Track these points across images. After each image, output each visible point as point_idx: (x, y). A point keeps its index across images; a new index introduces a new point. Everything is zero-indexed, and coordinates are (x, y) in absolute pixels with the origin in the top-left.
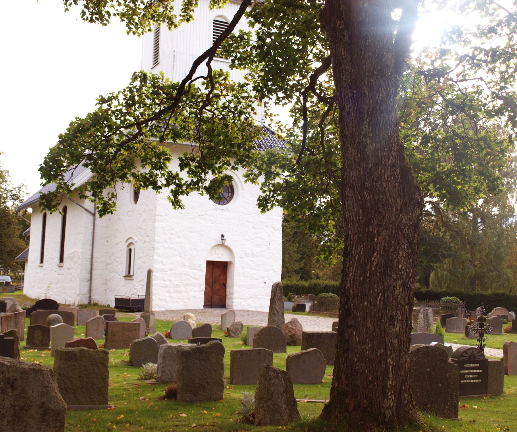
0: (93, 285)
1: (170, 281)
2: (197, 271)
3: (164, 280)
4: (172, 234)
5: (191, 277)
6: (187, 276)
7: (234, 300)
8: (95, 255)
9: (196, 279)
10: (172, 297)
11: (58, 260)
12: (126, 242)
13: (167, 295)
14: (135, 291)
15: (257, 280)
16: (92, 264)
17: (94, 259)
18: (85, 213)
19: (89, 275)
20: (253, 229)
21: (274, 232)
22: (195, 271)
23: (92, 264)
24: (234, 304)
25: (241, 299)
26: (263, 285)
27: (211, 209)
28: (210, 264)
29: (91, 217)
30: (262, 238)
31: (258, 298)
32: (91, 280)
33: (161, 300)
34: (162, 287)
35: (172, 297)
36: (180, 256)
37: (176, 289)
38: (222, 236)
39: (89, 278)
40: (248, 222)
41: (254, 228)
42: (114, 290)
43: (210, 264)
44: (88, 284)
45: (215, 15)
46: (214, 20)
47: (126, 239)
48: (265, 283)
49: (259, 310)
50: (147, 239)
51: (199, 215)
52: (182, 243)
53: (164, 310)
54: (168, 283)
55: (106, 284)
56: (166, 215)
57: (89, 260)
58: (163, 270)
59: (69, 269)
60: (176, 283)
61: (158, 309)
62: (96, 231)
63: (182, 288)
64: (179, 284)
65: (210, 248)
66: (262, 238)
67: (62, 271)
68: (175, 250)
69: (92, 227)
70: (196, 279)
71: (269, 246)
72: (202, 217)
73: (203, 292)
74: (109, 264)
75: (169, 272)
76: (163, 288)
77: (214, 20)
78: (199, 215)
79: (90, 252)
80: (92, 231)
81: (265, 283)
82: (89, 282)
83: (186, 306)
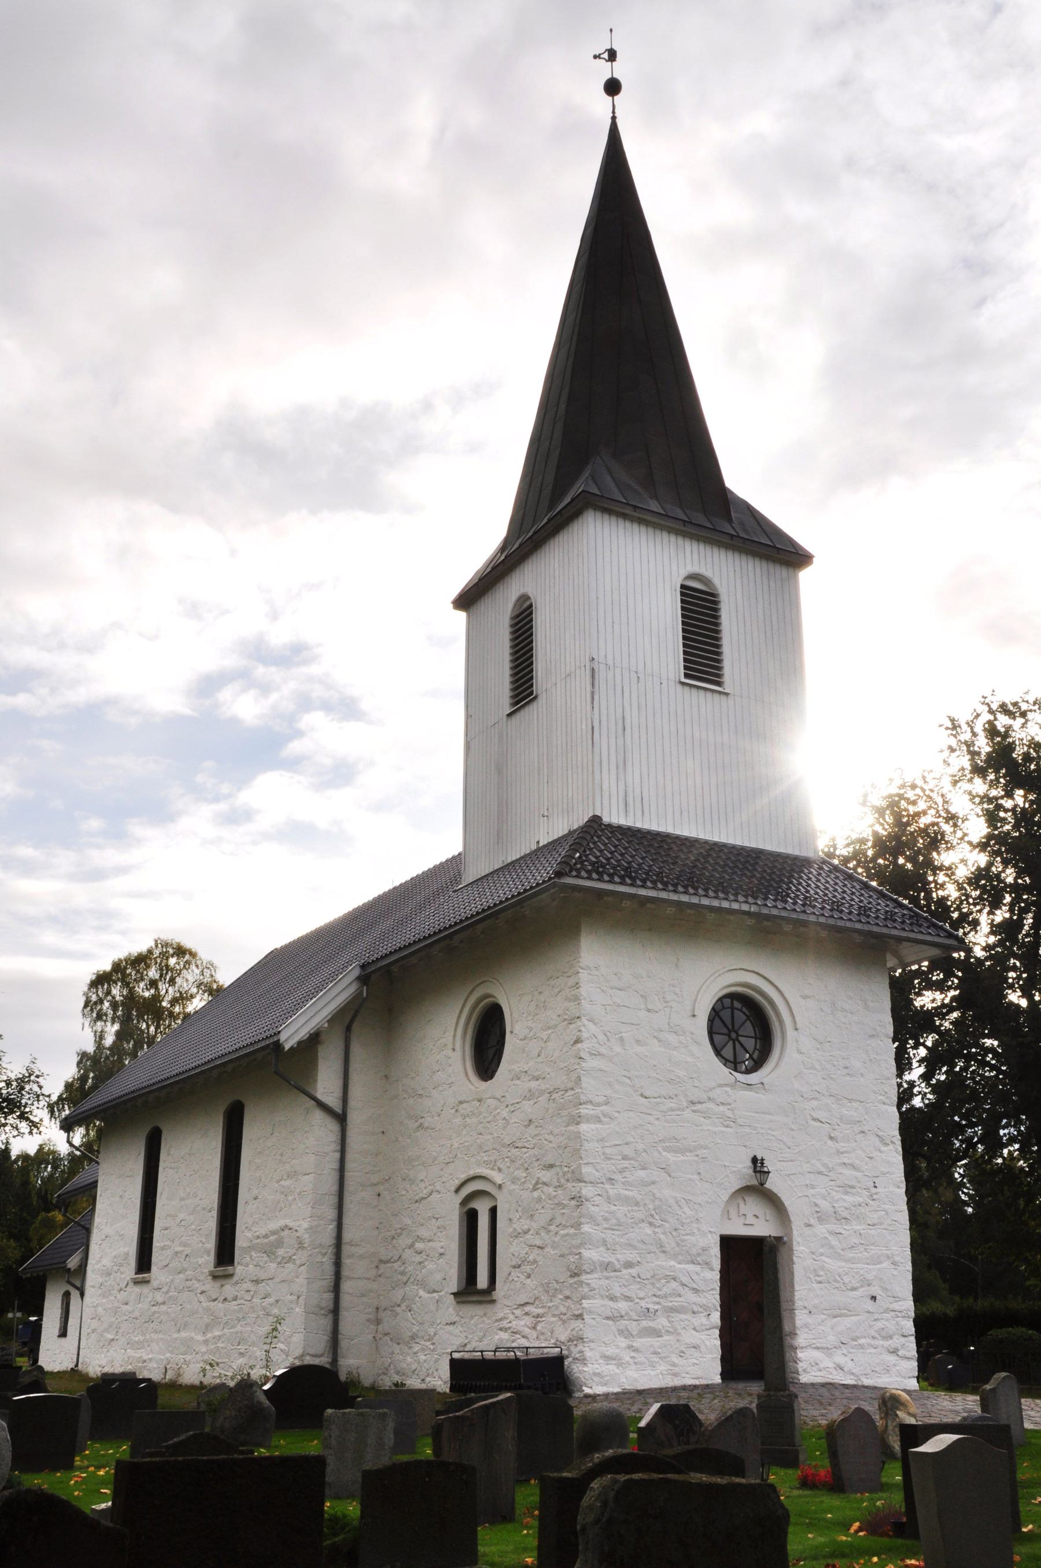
0: (344, 1327)
1: (628, 1298)
2: (698, 1268)
3: (613, 1298)
4: (625, 1158)
5: (683, 1285)
6: (674, 1285)
7: (800, 1354)
8: (347, 1236)
9: (696, 1291)
10: (636, 1350)
11: (211, 1259)
12: (457, 1191)
13: (623, 1342)
14: (504, 1336)
16: (338, 1264)
17: (346, 1249)
18: (319, 1115)
19: (331, 1296)
20: (830, 1142)
21: (883, 1148)
22: (691, 1267)
23: (338, 1264)
24: (801, 1366)
25: (817, 1348)
26: (870, 1305)
27: (720, 1086)
28: (728, 1243)
29: (333, 1126)
30: (853, 1167)
31: (861, 1346)
32: (335, 1311)
33: (607, 1358)
34: (607, 1318)
35: (636, 1350)
36: (651, 1224)
37: (645, 1324)
39: (331, 1306)
40: (815, 1119)
41: (831, 1138)
42: (413, 1338)
43: (728, 1243)
44: (326, 1322)
45: (684, 573)
47: (457, 1182)
48: (874, 1298)
49: (867, 1382)
50: (546, 1176)
51: (693, 1103)
52: (654, 1183)
53: (617, 1390)
54: (622, 1306)
55: (378, 1322)
56: (607, 1103)
57: (331, 1250)
58: (607, 1266)
59: (257, 1282)
60: (643, 1304)
61: (599, 1390)
62: (349, 1165)
63: (661, 1322)
64: (651, 1306)
65: (725, 1196)
66: (853, 1167)
67: (229, 1289)
68: (637, 1204)
69: (338, 1155)
71: (874, 1190)
72: (698, 1107)
73: (717, 1332)
74: (385, 1262)
75: (625, 1271)
76: (610, 1322)
77: (683, 587)
78: (693, 1103)
79: (332, 1227)
80: (336, 1165)
81: (874, 1298)
82: (331, 1316)
83: (675, 1375)
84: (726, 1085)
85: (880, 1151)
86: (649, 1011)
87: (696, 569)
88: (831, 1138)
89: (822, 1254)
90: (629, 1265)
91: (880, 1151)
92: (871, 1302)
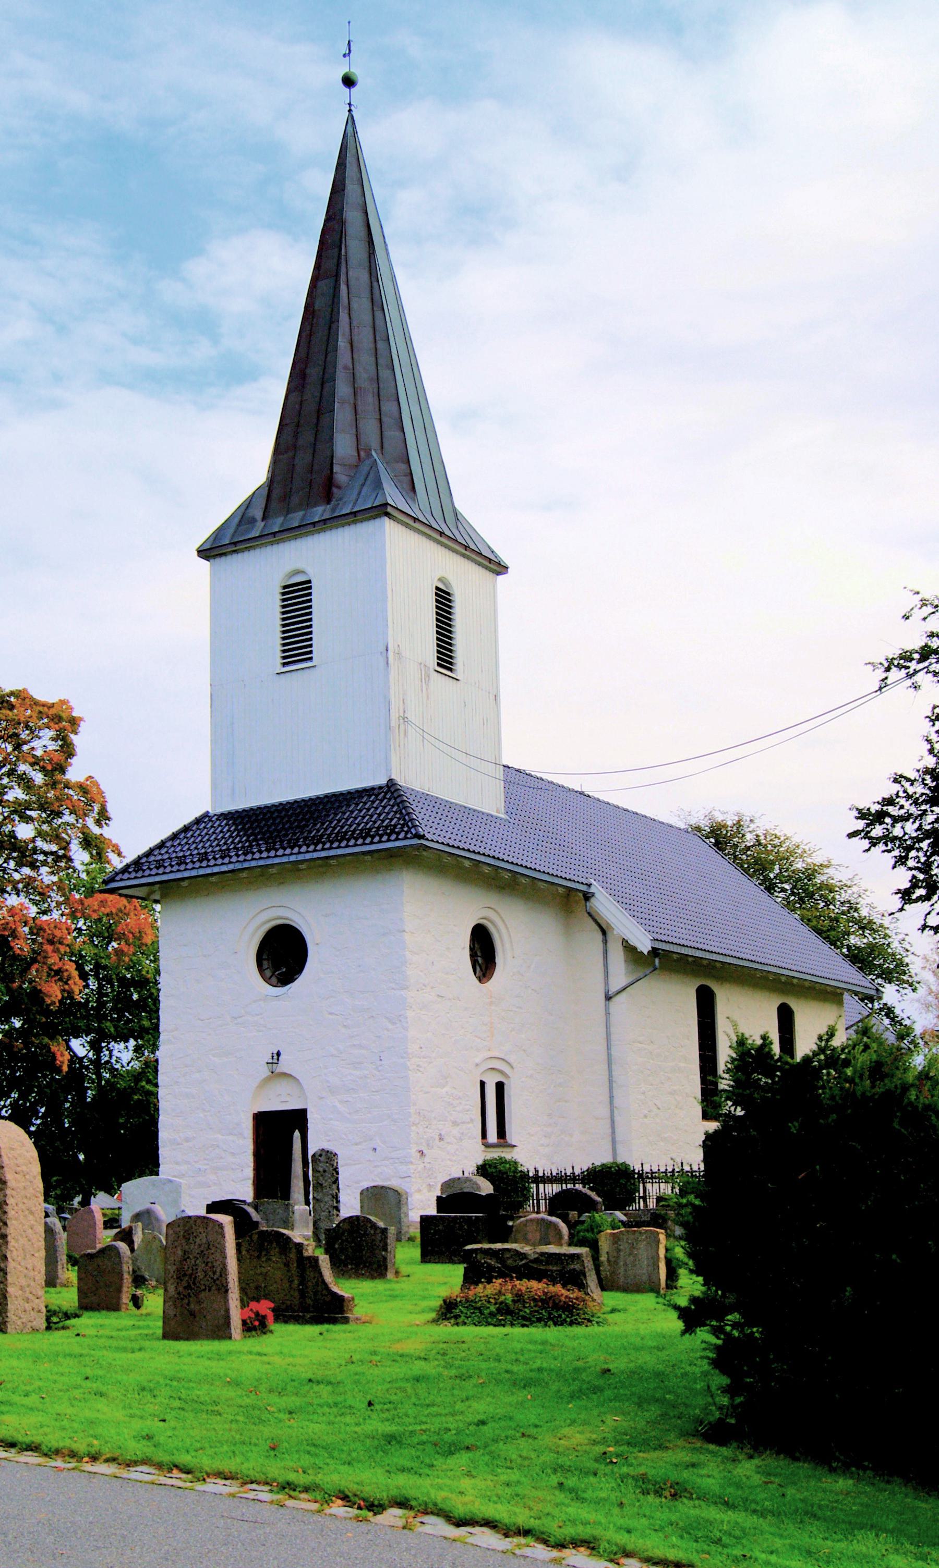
1: (188, 1163)
3: (177, 1163)
9: (233, 1154)
10: (193, 1197)
15: (357, 1144)
21: (390, 1026)
22: (231, 1138)
27: (255, 1001)
35: (193, 1197)
36: (204, 1110)
38: (278, 1054)
40: (331, 1014)
41: (345, 1026)
46: (285, 587)
51: (236, 1018)
56: (176, 1029)
70: (233, 1154)
71: (380, 1063)
72: (239, 1020)
73: (250, 1182)
78: (236, 1018)
81: (375, 1149)
84: (260, 1000)
85: (388, 1030)
86: (205, 956)
87: (289, 568)
88: (345, 1026)
89: (331, 1119)
90: (187, 1140)
91: (388, 1030)
92: (372, 1153)
